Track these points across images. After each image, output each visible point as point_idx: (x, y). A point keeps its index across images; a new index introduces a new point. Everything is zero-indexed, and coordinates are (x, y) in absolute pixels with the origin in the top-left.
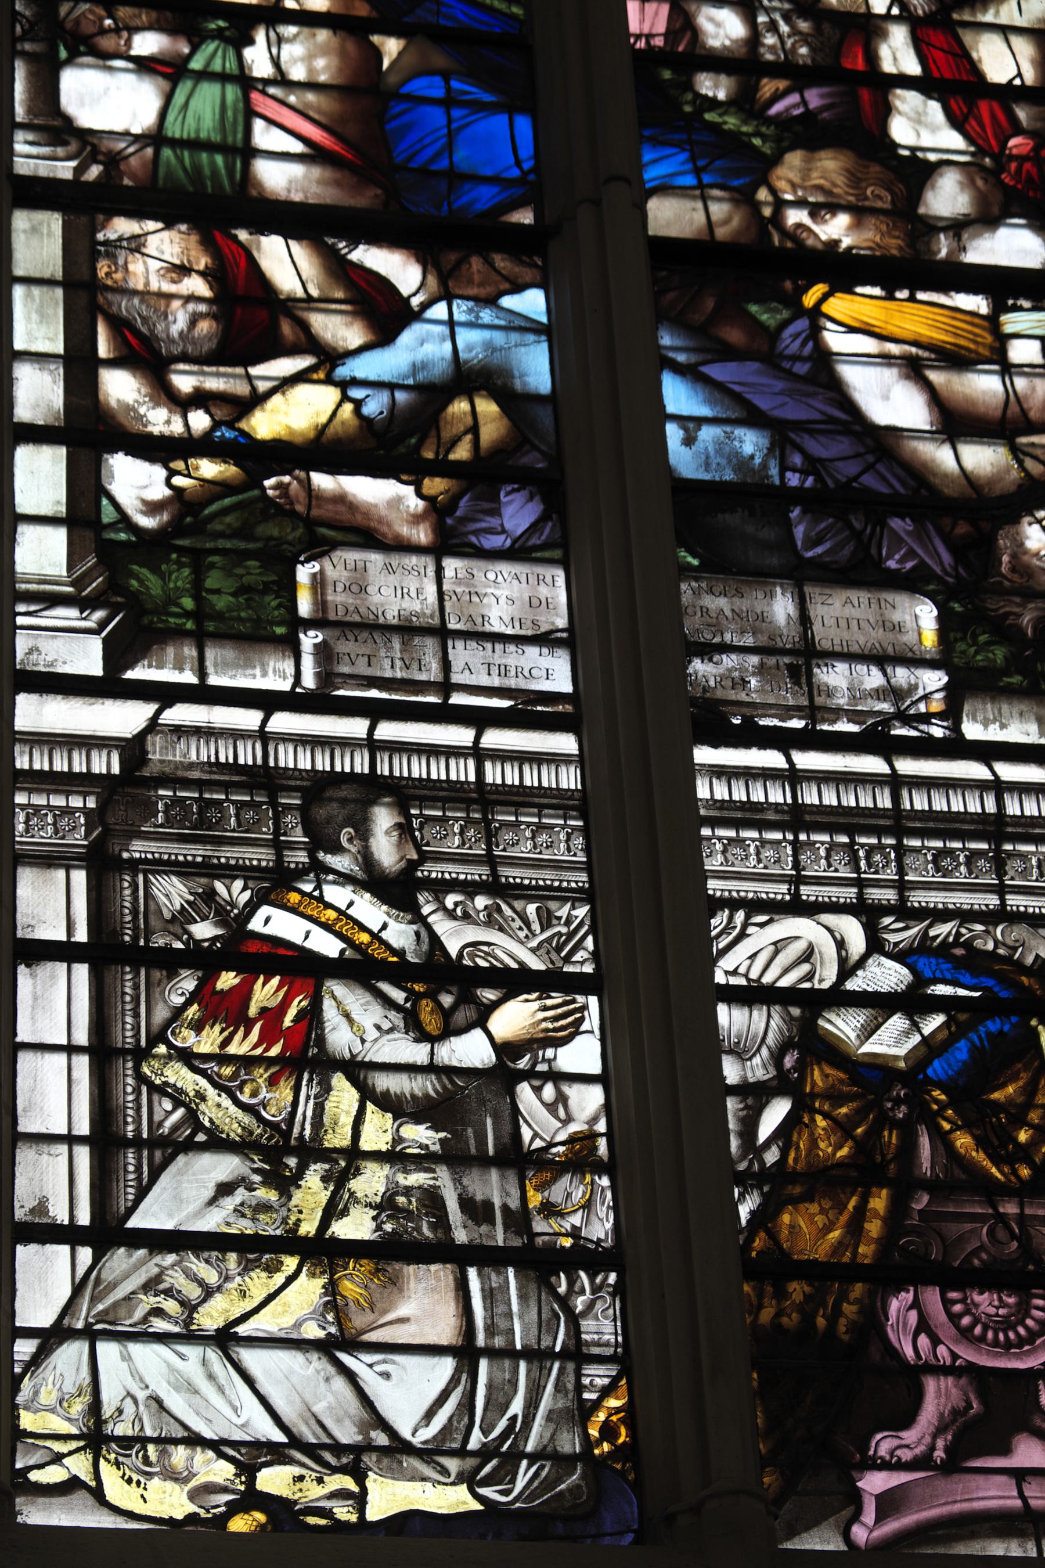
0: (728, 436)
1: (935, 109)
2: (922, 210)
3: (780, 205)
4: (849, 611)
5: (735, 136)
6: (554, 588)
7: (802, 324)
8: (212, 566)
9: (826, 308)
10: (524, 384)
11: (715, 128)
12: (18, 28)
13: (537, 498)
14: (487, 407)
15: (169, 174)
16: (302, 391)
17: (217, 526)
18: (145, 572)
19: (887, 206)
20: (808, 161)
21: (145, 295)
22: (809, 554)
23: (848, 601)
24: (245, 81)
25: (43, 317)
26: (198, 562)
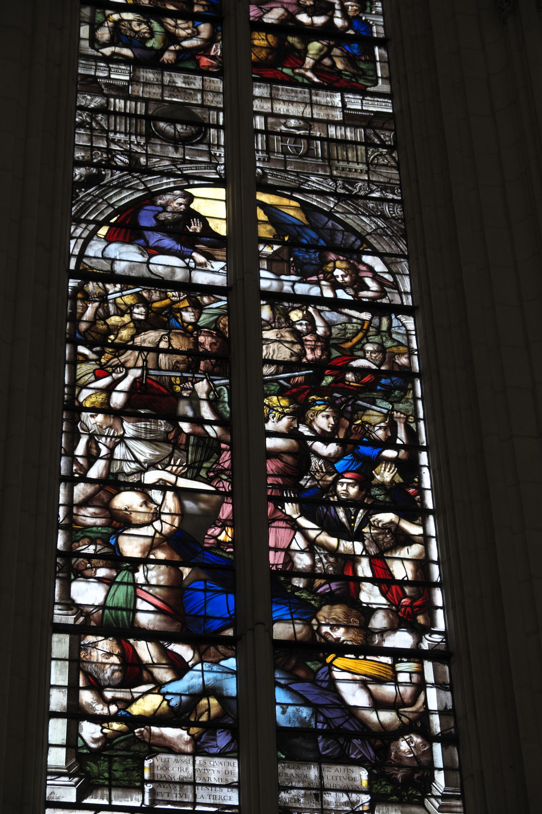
0: (298, 710)
1: (376, 589)
2: (370, 626)
3: (320, 625)
4: (337, 774)
5: (305, 600)
6: (233, 767)
7: (326, 669)
8: (115, 761)
9: (334, 663)
10: (227, 693)
11: (298, 597)
12: (58, 568)
13: (230, 734)
14: (213, 701)
15: (107, 619)
16: (150, 697)
17: (117, 747)
18: (92, 764)
19: (358, 625)
20: (330, 609)
21: (97, 663)
22: (324, 753)
23: (337, 770)
24: (135, 585)
25: (61, 672)
26: (110, 760)
